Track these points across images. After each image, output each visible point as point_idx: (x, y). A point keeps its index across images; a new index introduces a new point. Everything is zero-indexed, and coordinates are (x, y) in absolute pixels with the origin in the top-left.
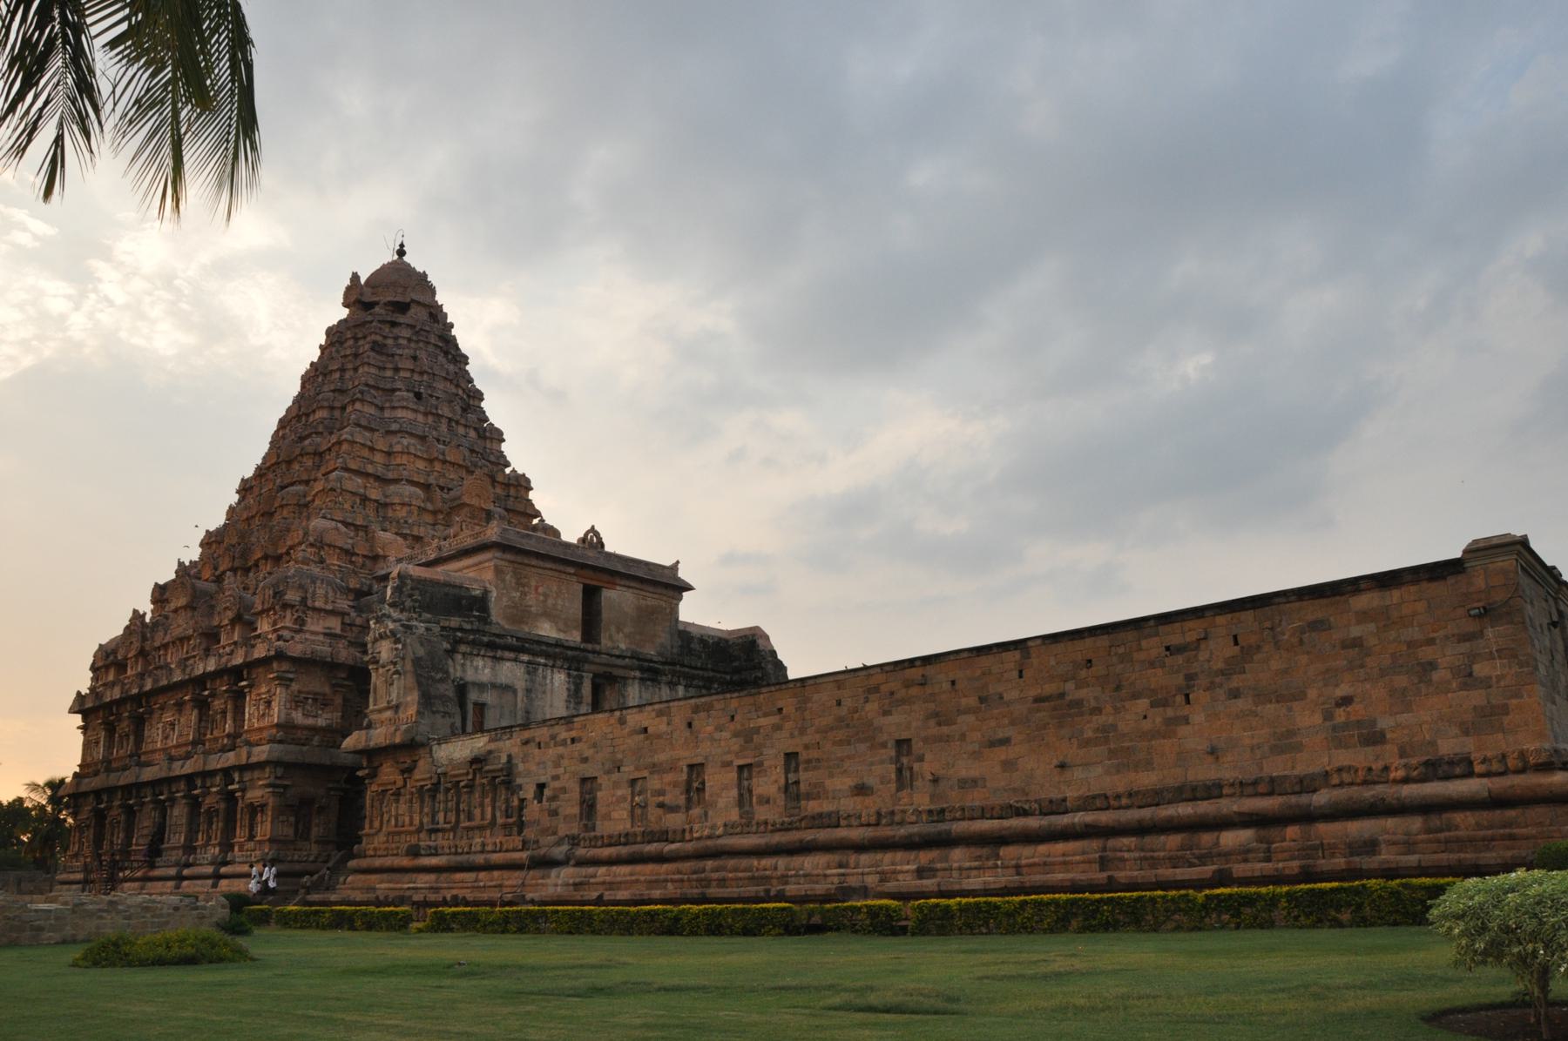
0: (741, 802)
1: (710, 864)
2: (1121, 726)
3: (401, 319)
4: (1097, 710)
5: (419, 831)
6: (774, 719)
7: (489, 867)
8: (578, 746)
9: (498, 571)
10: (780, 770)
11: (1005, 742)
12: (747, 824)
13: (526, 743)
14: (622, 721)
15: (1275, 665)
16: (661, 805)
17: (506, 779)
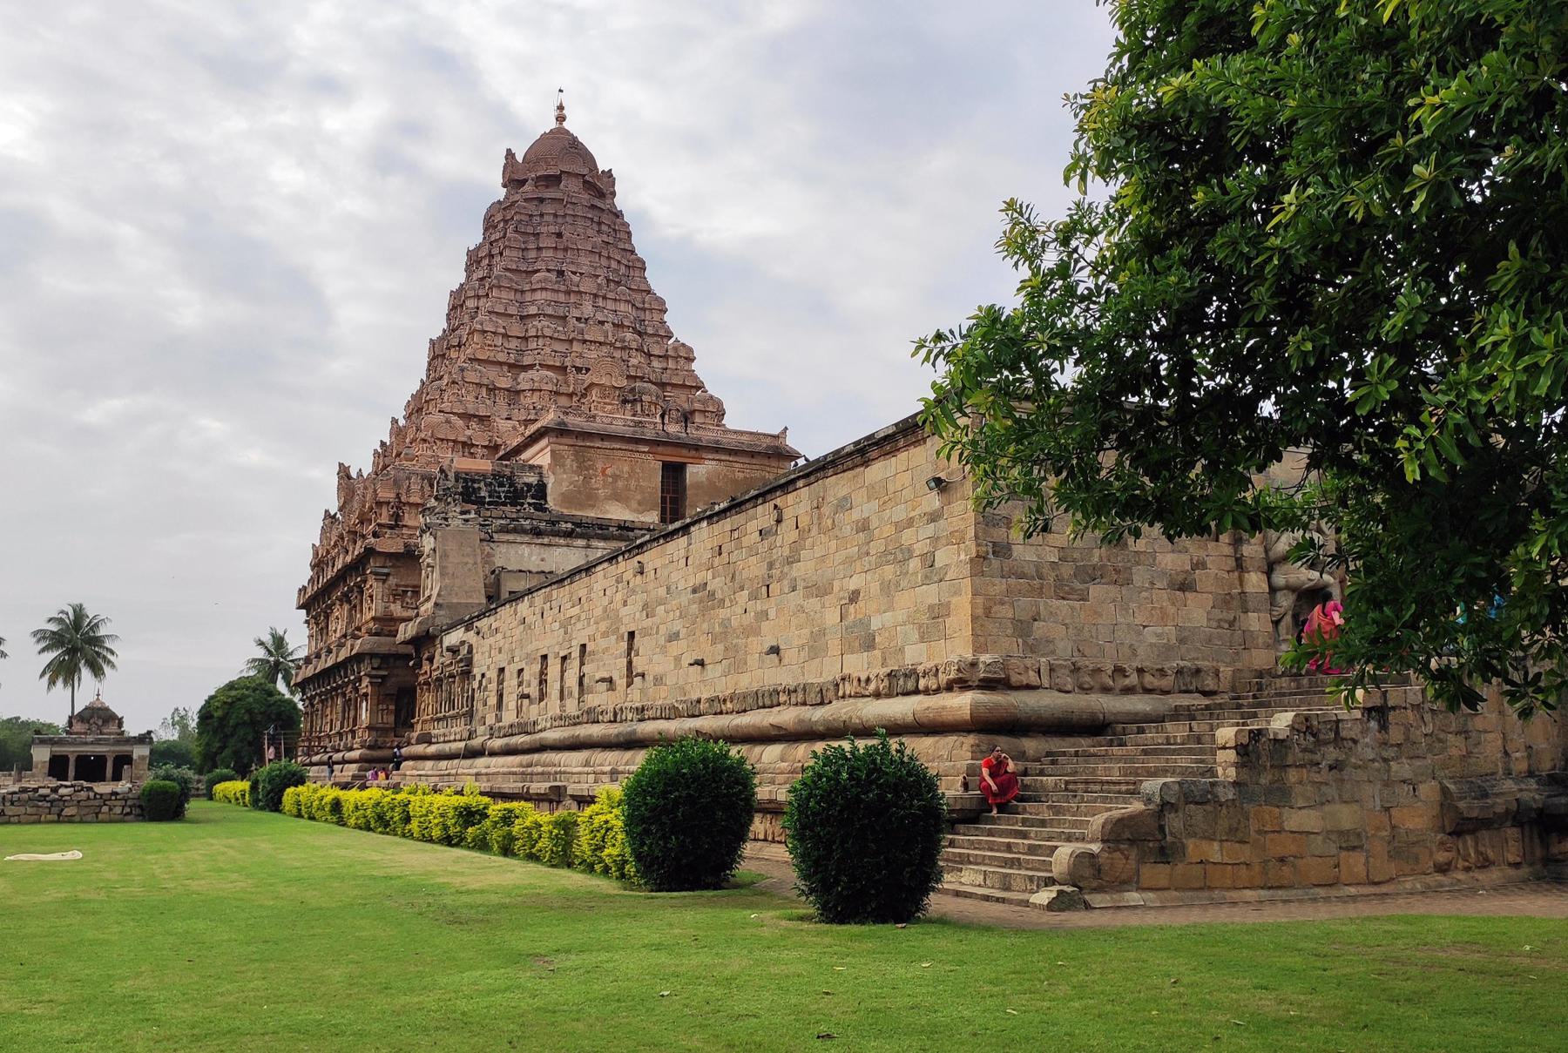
0: (562, 698)
1: (536, 756)
8: (499, 636)
12: (563, 720)
16: (527, 696)
17: (467, 674)
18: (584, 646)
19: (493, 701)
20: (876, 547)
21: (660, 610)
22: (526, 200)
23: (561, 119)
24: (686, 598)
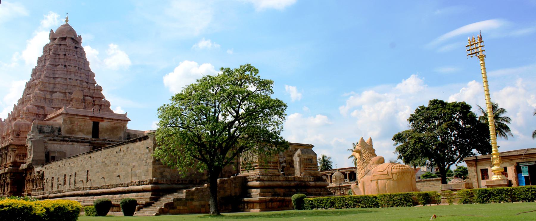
2: (111, 169)
15: (127, 157)
18: (76, 173)
19: (50, 185)
20: (138, 158)
24: (100, 164)
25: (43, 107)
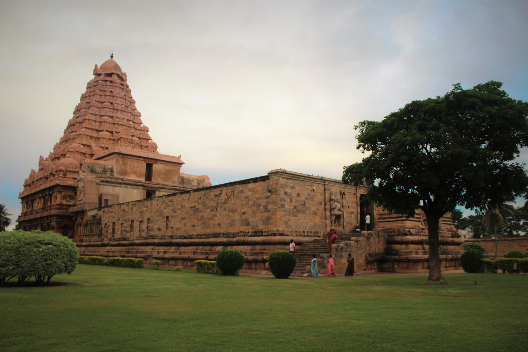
0: (140, 231)
1: (131, 247)
3: (109, 79)
4: (201, 211)
5: (83, 235)
6: (146, 209)
7: (94, 246)
8: (113, 213)
9: (117, 160)
10: (146, 223)
11: (185, 218)
12: (140, 237)
13: (104, 212)
14: (120, 208)
15: (233, 202)
16: (126, 231)
17: (99, 222)
19: (110, 231)
20: (251, 203)
21: (179, 211)
22: (102, 80)
23: (112, 57)
24: (188, 209)
25: (89, 146)
